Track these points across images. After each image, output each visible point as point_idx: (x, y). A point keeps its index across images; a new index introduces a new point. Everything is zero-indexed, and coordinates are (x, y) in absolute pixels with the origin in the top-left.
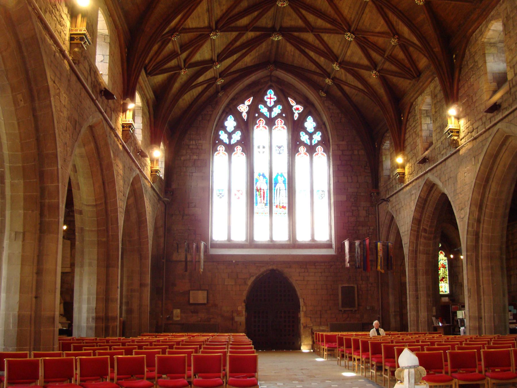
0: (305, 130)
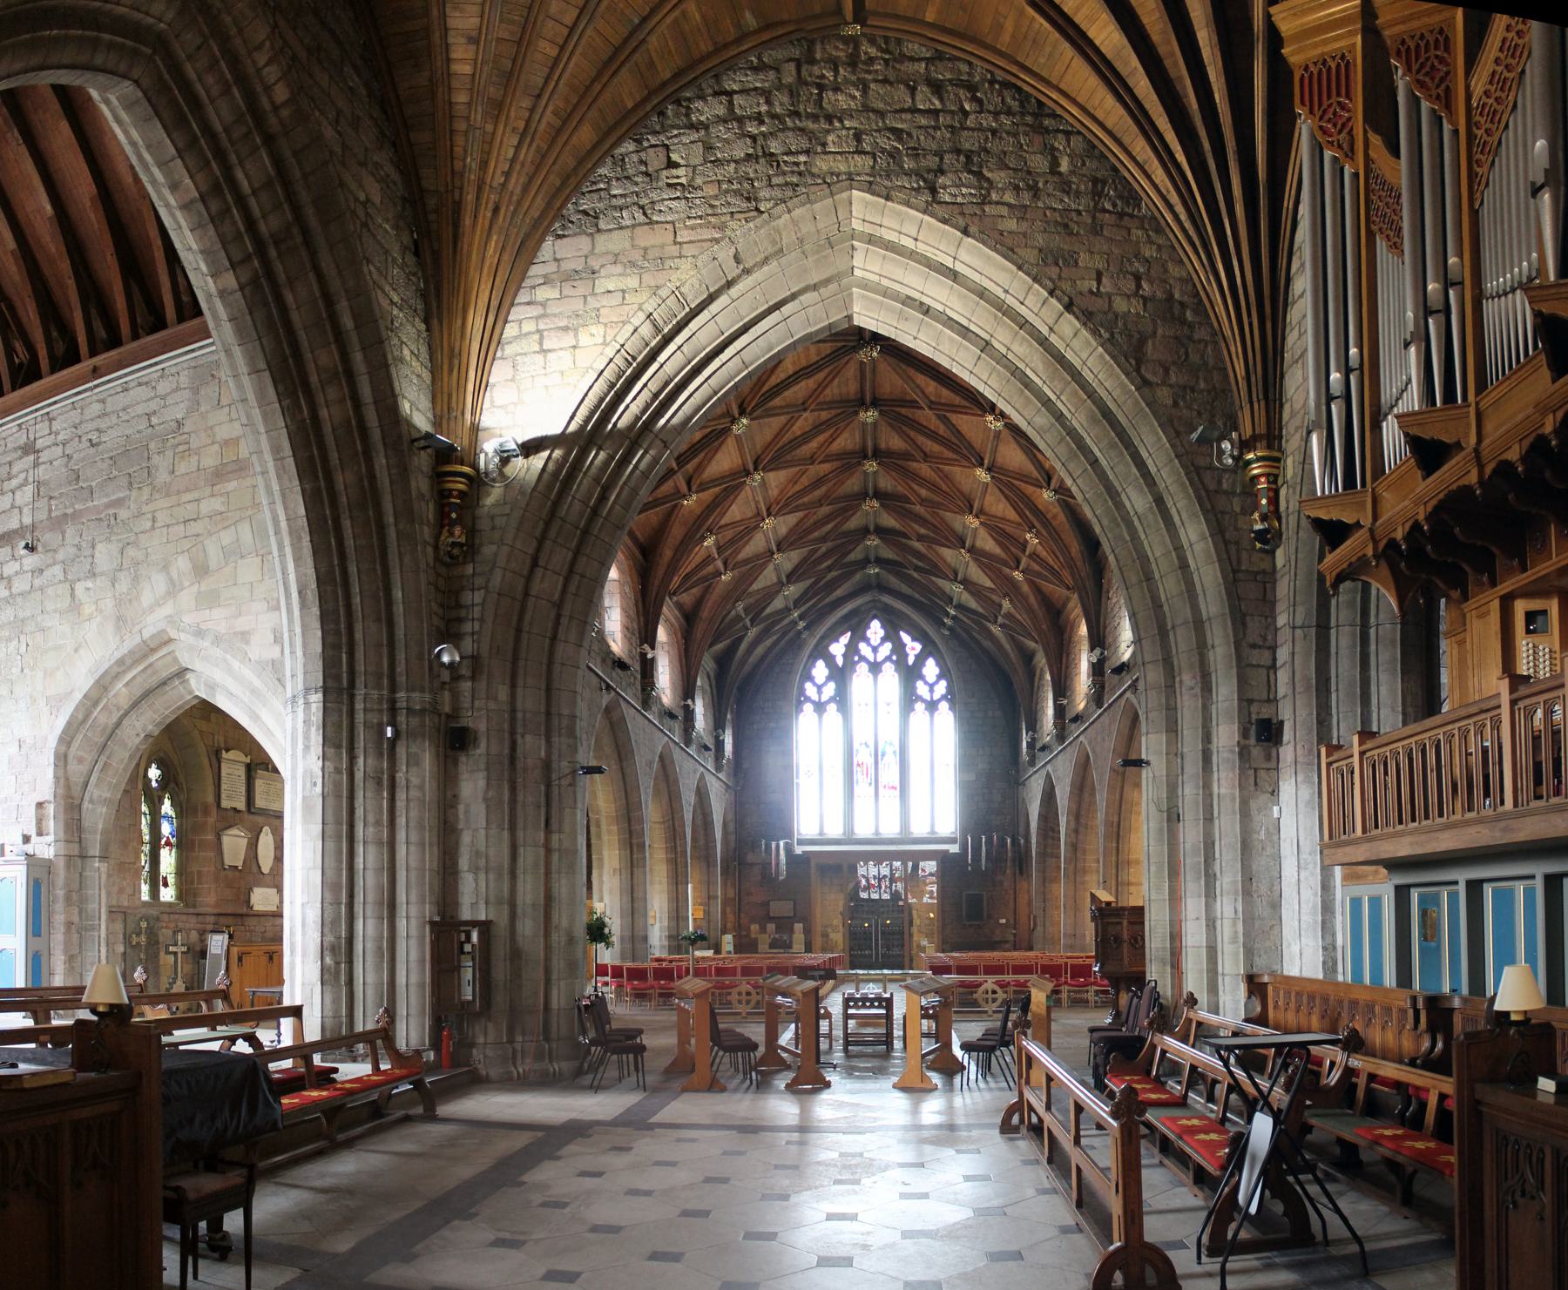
0: (922, 677)
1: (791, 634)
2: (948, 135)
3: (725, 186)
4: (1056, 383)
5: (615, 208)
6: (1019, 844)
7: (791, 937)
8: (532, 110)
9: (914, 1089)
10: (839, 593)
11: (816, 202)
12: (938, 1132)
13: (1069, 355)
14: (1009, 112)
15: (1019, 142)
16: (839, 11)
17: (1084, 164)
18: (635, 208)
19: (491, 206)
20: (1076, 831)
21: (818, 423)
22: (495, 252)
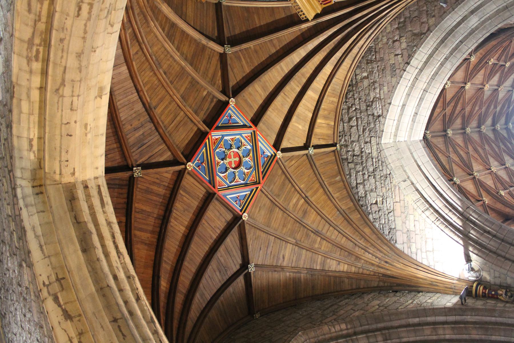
2: (363, 114)
3: (383, 185)
4: (434, 63)
5: (388, 222)
8: (359, 247)
13: (424, 60)
14: (353, 95)
16: (334, 151)
17: (363, 68)
18: (389, 215)
19: (385, 264)
22: (400, 265)
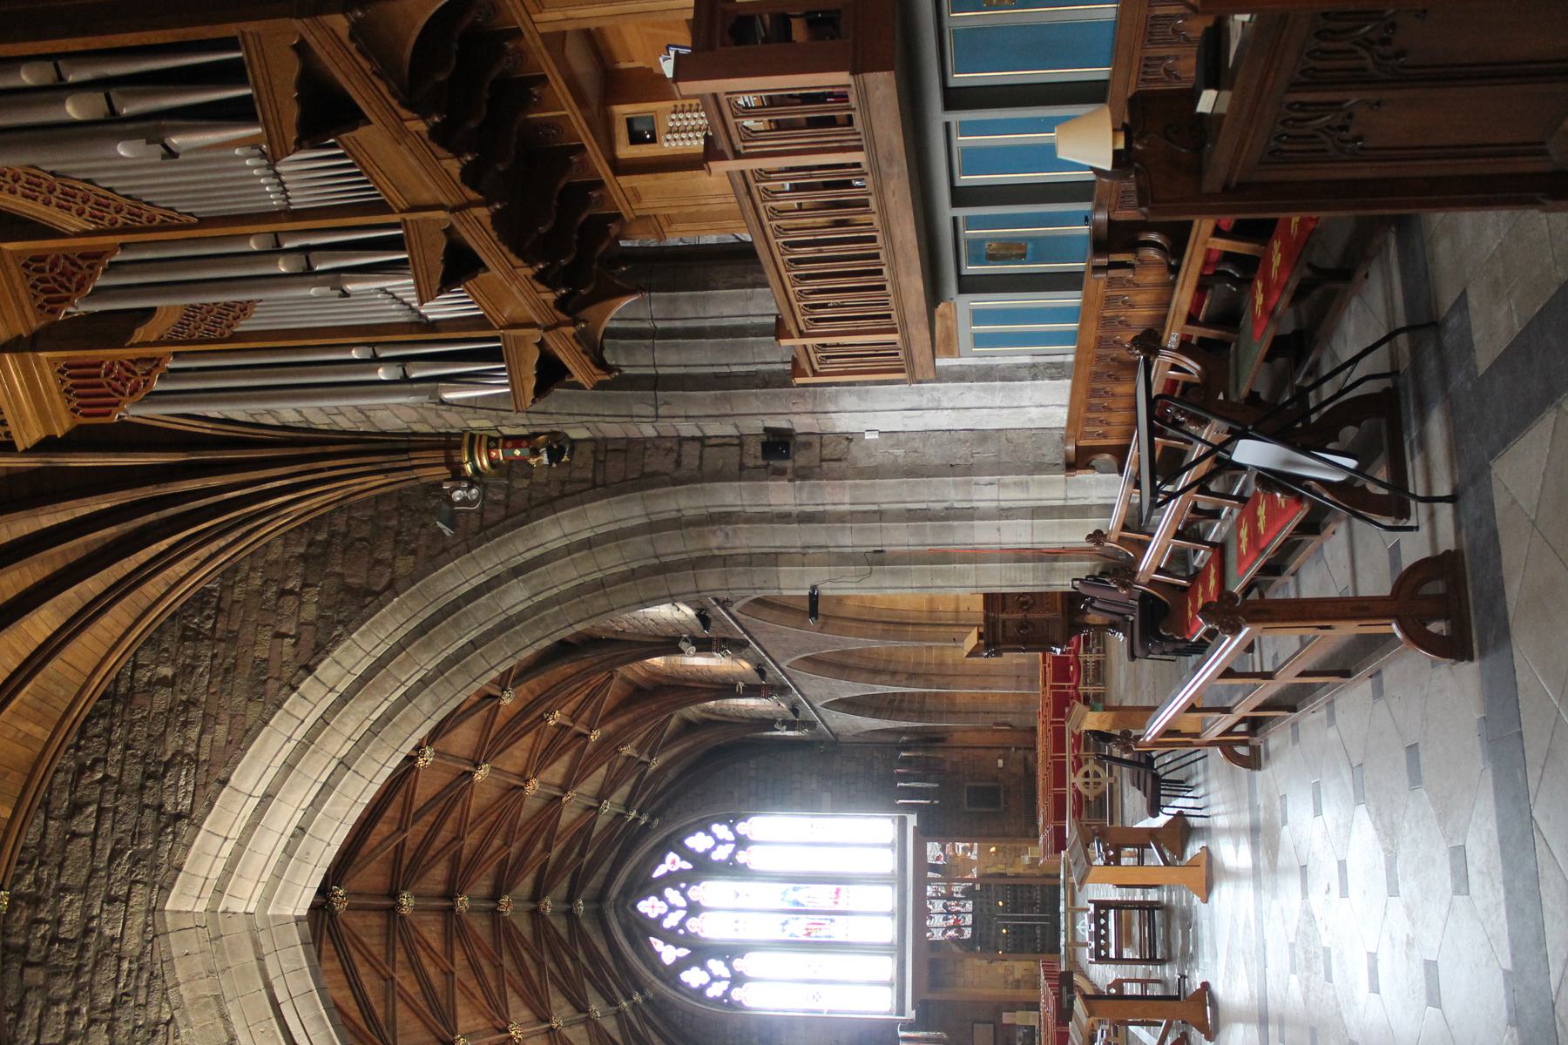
0: (708, 853)
1: (647, 1011)
2: (125, 798)
4: (387, 686)
6: (908, 742)
7: (1020, 1027)
9: (1208, 877)
10: (603, 949)
11: (170, 952)
12: (1262, 848)
13: (359, 671)
14: (109, 730)
15: (140, 720)
17: (166, 650)
20: (894, 673)
21: (408, 965)
